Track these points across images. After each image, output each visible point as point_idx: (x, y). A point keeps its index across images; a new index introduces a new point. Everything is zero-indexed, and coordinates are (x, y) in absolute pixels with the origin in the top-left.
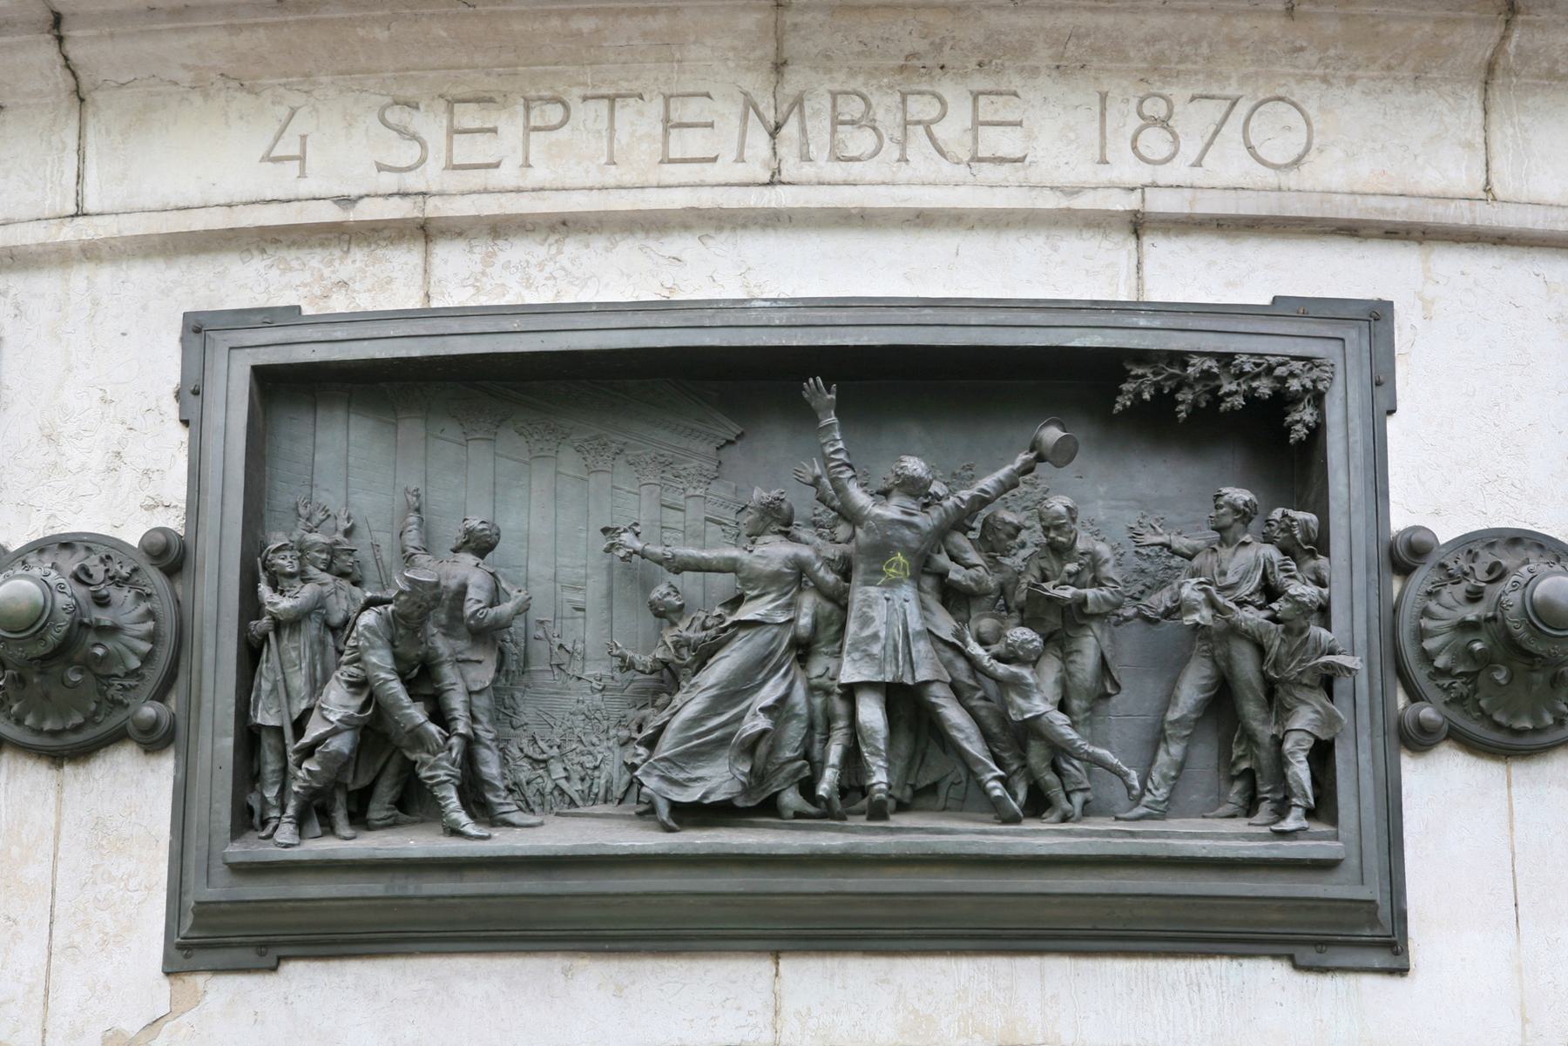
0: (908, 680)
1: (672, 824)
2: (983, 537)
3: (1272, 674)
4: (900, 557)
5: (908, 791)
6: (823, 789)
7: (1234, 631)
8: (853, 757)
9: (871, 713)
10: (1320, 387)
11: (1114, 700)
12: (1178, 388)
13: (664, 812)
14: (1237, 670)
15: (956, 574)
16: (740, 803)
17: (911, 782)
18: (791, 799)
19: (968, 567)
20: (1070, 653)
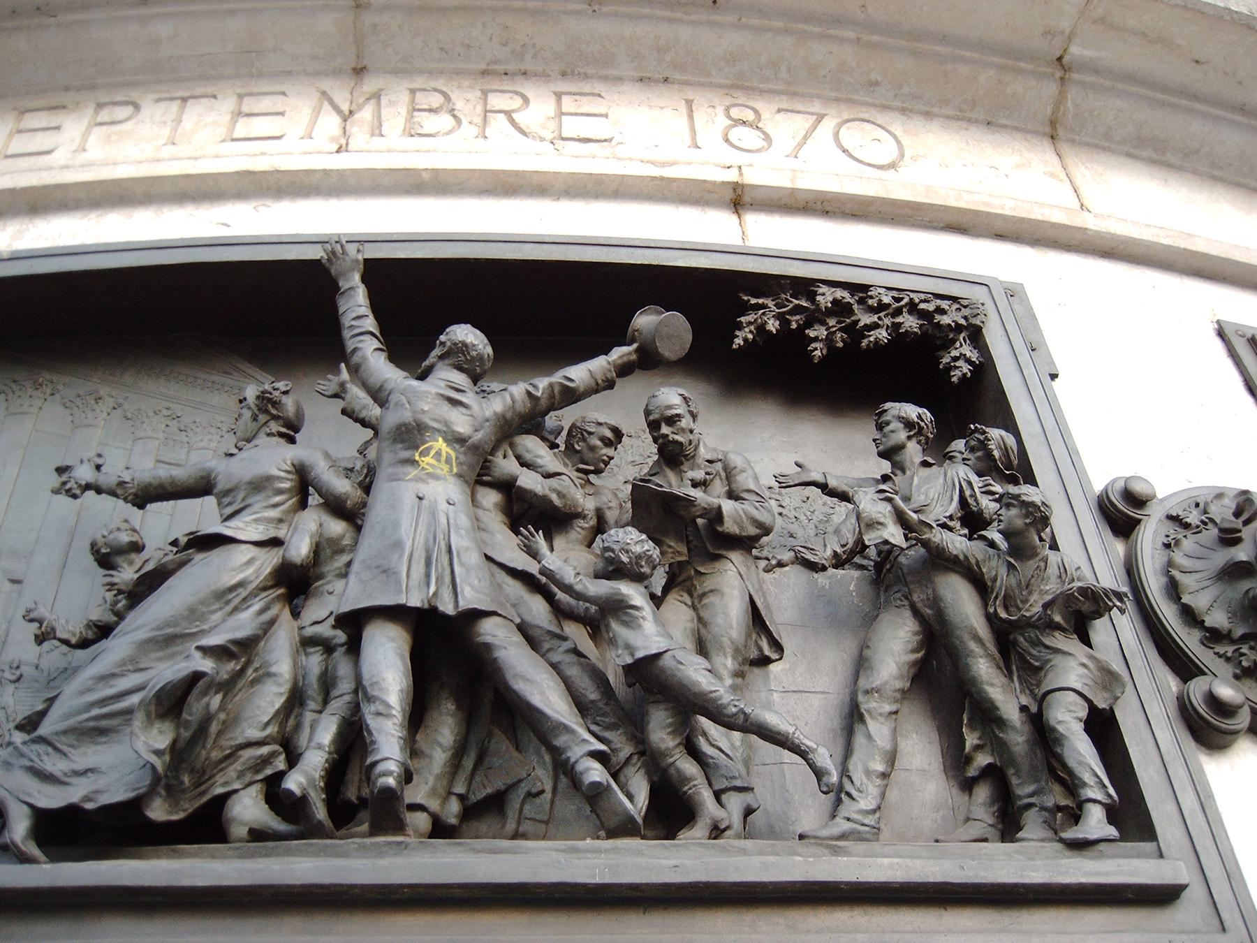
0: (447, 608)
1: (33, 849)
2: (569, 446)
3: (1003, 615)
4: (440, 444)
5: (454, 807)
7: (939, 560)
10: (977, 322)
11: (774, 668)
12: (809, 324)
13: (19, 828)
14: (951, 614)
15: (528, 481)
16: (158, 812)
17: (460, 788)
18: (249, 808)
19: (548, 476)
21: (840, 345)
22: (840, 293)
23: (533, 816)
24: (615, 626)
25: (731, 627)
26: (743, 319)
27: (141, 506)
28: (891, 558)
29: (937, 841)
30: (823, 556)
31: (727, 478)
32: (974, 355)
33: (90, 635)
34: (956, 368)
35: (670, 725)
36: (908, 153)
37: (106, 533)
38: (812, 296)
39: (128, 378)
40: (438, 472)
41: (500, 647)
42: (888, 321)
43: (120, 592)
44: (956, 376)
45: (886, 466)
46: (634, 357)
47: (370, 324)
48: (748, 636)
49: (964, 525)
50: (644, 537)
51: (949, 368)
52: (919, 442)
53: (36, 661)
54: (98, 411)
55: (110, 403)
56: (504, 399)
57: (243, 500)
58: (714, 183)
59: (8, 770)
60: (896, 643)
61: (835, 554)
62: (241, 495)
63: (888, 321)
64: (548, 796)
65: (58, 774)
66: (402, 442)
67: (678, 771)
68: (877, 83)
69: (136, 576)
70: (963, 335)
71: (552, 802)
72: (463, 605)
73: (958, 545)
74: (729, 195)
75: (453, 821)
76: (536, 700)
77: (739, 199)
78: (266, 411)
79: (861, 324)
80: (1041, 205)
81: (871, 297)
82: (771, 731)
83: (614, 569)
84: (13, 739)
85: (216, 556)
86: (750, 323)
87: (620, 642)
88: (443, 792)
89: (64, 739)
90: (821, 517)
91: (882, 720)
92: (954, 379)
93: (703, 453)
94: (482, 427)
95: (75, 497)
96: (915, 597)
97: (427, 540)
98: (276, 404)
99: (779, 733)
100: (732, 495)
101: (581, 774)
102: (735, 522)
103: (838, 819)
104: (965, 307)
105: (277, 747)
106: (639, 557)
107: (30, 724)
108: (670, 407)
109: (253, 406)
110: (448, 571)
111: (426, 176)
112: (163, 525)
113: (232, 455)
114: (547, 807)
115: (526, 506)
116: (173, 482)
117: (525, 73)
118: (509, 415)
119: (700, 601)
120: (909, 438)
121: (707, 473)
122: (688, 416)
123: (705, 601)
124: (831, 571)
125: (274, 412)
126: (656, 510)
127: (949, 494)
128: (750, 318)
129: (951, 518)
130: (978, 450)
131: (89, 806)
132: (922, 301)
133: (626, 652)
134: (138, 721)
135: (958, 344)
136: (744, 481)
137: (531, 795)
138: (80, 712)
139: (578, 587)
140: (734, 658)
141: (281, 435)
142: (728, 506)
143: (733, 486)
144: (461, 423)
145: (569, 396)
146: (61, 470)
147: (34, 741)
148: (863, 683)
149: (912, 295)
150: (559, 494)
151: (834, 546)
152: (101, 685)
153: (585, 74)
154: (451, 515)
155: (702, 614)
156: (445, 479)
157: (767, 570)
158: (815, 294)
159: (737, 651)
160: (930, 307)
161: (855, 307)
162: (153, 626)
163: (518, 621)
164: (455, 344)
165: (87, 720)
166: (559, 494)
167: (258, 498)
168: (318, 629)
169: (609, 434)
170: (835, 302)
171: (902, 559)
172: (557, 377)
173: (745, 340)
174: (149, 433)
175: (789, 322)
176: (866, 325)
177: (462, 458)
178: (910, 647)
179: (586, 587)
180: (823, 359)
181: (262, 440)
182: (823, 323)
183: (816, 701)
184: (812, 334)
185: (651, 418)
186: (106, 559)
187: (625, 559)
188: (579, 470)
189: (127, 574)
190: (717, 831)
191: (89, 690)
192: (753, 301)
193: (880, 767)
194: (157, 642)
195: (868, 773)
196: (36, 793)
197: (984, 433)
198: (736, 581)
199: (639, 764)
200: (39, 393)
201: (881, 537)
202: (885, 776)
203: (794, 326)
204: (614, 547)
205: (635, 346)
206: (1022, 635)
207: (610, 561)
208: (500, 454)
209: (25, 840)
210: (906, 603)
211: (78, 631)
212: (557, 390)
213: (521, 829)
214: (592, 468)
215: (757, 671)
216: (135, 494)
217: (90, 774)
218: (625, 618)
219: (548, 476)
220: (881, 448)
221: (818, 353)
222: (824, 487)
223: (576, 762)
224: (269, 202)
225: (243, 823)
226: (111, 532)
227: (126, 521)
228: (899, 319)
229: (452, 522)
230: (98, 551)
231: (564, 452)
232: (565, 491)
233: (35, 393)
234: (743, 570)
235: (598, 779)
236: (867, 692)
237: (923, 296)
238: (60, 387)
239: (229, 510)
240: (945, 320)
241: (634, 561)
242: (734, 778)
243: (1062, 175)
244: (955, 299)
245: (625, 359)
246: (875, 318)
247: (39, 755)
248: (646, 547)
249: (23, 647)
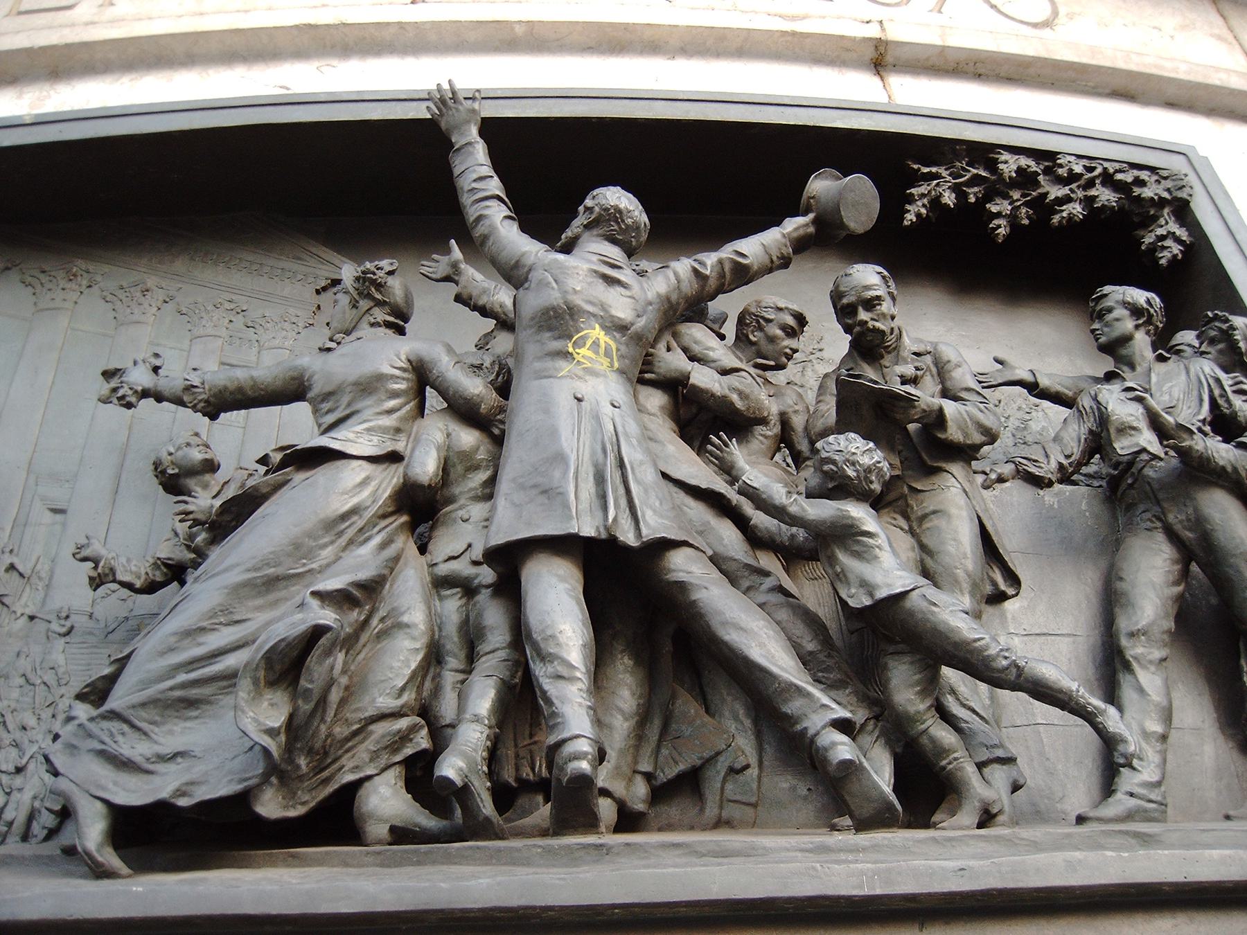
0: (628, 537)
1: (111, 858)
4: (596, 333)
5: (641, 789)
6: (450, 768)
7: (1198, 472)
8: (523, 703)
9: (558, 603)
10: (1183, 194)
11: (1010, 606)
12: (988, 197)
13: (92, 831)
14: (1221, 537)
15: (703, 378)
16: (270, 806)
17: (645, 766)
18: (387, 800)
19: (725, 372)
20: (924, 517)
21: (1026, 222)
22: (1024, 161)
23: (738, 797)
24: (843, 557)
25: (965, 557)
26: (913, 191)
27: (213, 417)
28: (1133, 470)
29: (1228, 817)
30: (1047, 469)
31: (939, 374)
32: (1182, 233)
33: (159, 578)
34: (1164, 248)
35: (918, 683)
36: (1062, 11)
37: (172, 450)
38: (992, 165)
39: (180, 265)
40: (597, 367)
41: (699, 587)
42: (1081, 194)
43: (196, 522)
44: (1164, 258)
45: (1108, 364)
46: (811, 229)
47: (495, 186)
48: (983, 568)
49: (1216, 431)
50: (871, 445)
51: (1153, 249)
52: (1148, 333)
53: (89, 609)
54: (146, 305)
55: (161, 295)
56: (668, 278)
57: (349, 405)
58: (853, 39)
59: (72, 755)
60: (1152, 573)
61: (1061, 466)
62: (345, 399)
63: (1081, 194)
64: (753, 772)
65: (138, 759)
66: (550, 329)
67: (933, 740)
69: (218, 503)
70: (1166, 211)
71: (759, 777)
72: (648, 533)
73: (1224, 455)
74: (870, 53)
75: (640, 807)
76: (756, 654)
77: (880, 58)
78: (369, 296)
79: (1052, 197)
80: (1217, 70)
81: (1061, 166)
82: (1051, 688)
83: (837, 486)
84: (73, 713)
85: (322, 475)
86: (923, 196)
87: (851, 576)
88: (628, 772)
89: (143, 714)
90: (1017, 423)
91: (1153, 668)
92: (1163, 262)
93: (909, 344)
94: (645, 311)
95: (129, 406)
96: (1171, 518)
97: (593, 453)
98: (380, 286)
99: (1061, 691)
100: (945, 394)
101: (826, 749)
102: (960, 428)
103: (1119, 796)
104: (1165, 178)
105: (418, 719)
106: (868, 470)
107: (97, 693)
108: (867, 288)
109: (352, 290)
110: (622, 491)
111: (519, 30)
112: (241, 442)
113: (329, 350)
114: (755, 786)
115: (694, 410)
116: (255, 386)
118: (674, 297)
119: (920, 525)
120: (1137, 327)
121: (917, 369)
122: (888, 299)
123: (926, 525)
124: (1057, 487)
125: (379, 297)
126: (869, 409)
127: (1195, 393)
128: (923, 189)
129: (1203, 421)
130: (1220, 342)
131: (183, 802)
132: (1117, 171)
133: (862, 591)
134: (244, 687)
135: (1162, 221)
136: (963, 377)
137: (733, 771)
138: (161, 679)
139: (793, 509)
140: (972, 594)
141: (388, 325)
142: (950, 407)
143: (949, 384)
144: (621, 306)
145: (741, 275)
146: (108, 375)
147: (104, 717)
148: (1124, 624)
149: (1106, 164)
150: (741, 394)
151: (1057, 457)
152: (186, 642)
154: (618, 420)
155: (925, 541)
156: (605, 376)
157: (986, 487)
158: (996, 162)
159: (975, 587)
160: (1128, 177)
161: (1041, 178)
162: (249, 565)
163: (710, 553)
164: (606, 210)
165: (171, 689)
166: (741, 394)
167: (368, 402)
168: (454, 566)
169: (790, 321)
170: (1020, 171)
171: (1149, 472)
172: (727, 252)
173: (918, 215)
174: (210, 331)
175: (966, 195)
176: (1057, 198)
177: (623, 348)
178: (1171, 578)
179: (803, 510)
180: (1007, 238)
181: (365, 331)
182: (1006, 196)
183: (1064, 645)
184: (994, 209)
185: (845, 301)
186: (174, 482)
187: (851, 472)
188: (757, 366)
189: (205, 500)
190: (987, 818)
191: (171, 650)
192: (926, 170)
193: (1156, 727)
194: (255, 586)
195: (1146, 735)
196: (111, 786)
197: (1227, 321)
198: (961, 500)
199: (876, 733)
200: (73, 285)
201: (1138, 444)
202: (1164, 738)
203: (972, 199)
204: (837, 458)
205: (811, 216)
207: (828, 476)
208: (662, 346)
209: (100, 847)
210: (1159, 524)
211: (143, 572)
212: (727, 267)
213: (725, 814)
214: (772, 363)
215: (989, 611)
216: (207, 401)
217: (179, 760)
218: (856, 548)
219: (725, 372)
220: (1103, 339)
221: (1002, 231)
222: (1033, 388)
223: (817, 734)
224: (335, 62)
225: (381, 820)
226: (179, 448)
227: (197, 434)
228: (1093, 192)
229: (620, 429)
230: (163, 472)
231: (735, 344)
232: (747, 391)
233: (68, 285)
234: (967, 486)
235: (848, 757)
236: (1132, 635)
237: (1117, 166)
238: (99, 278)
239: (330, 419)
240: (1147, 193)
241: (863, 474)
242: (995, 746)
243: (1230, 37)
244: (1153, 170)
245: (801, 232)
246: (1066, 190)
247: (112, 735)
248: (876, 458)
249: (73, 592)
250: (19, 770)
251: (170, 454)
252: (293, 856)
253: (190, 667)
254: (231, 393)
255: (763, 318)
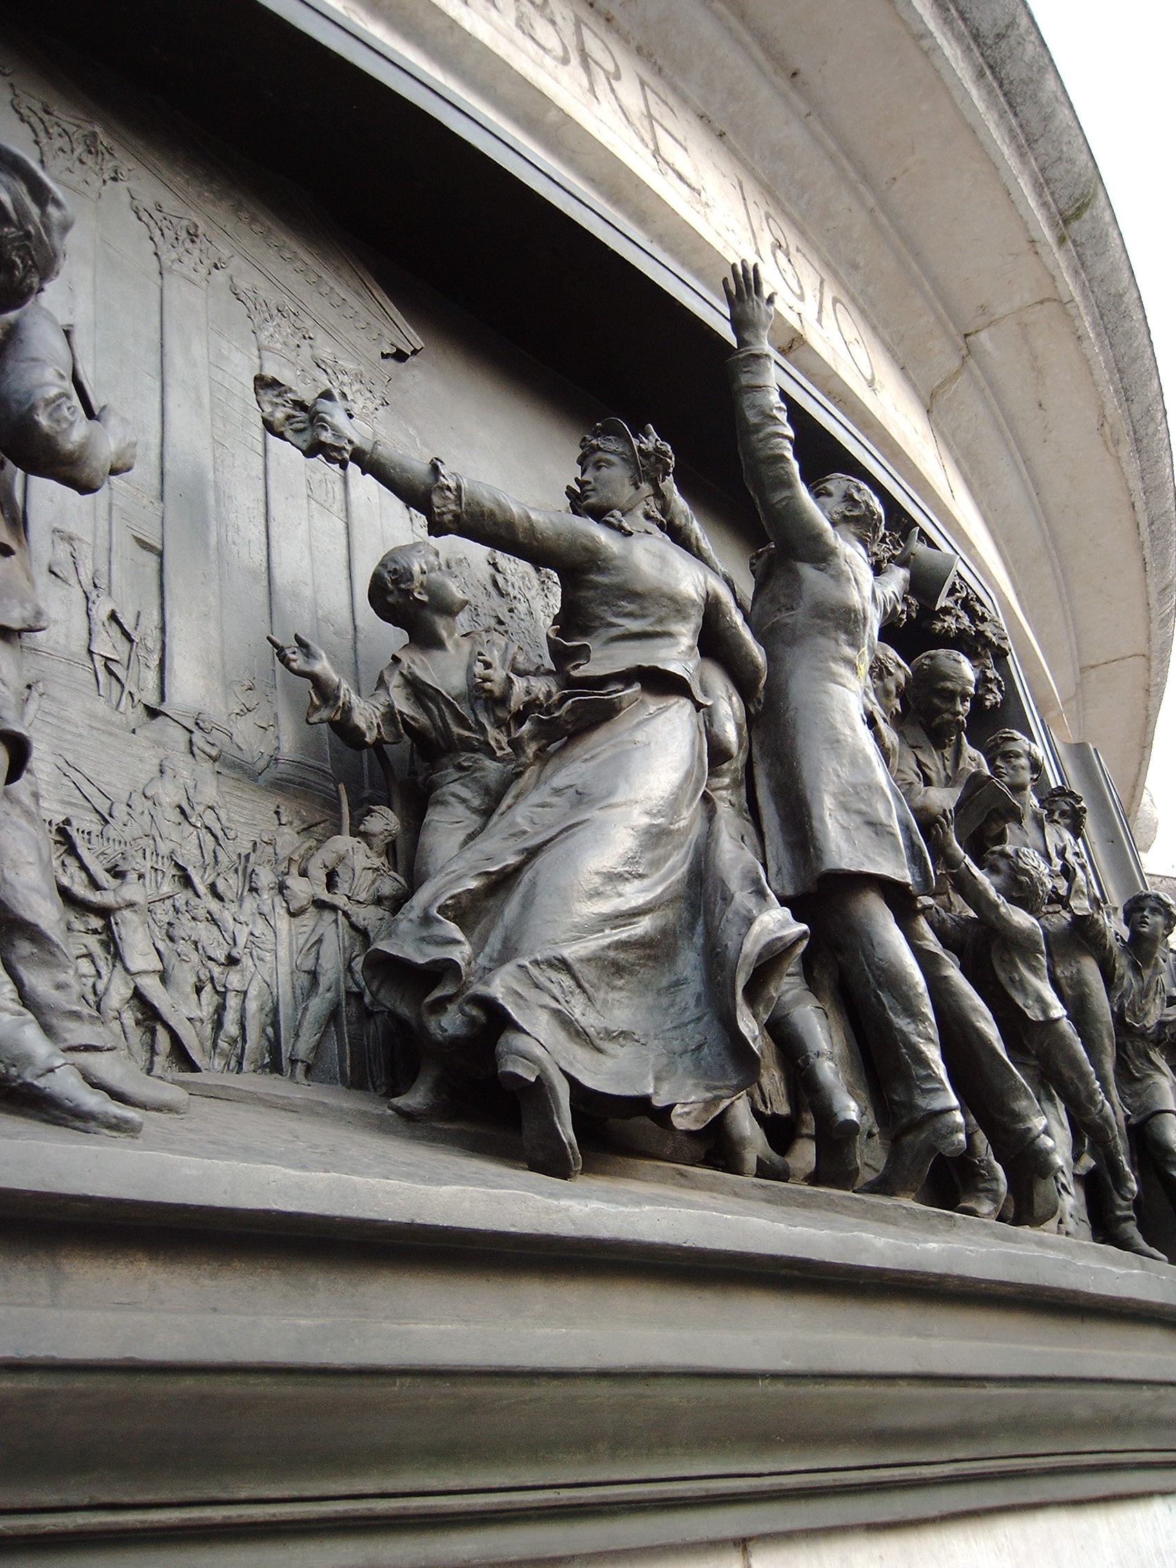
65: (591, 1031)
68: (855, 267)
92: (988, 703)
96: (1058, 971)
117: (608, 20)
133: (1036, 1006)
153: (660, 70)
206: (1132, 1042)
226: (432, 570)
233: (89, 160)
250: (232, 961)
251: (423, 572)
252: (682, 1174)
253: (618, 922)
254: (496, 523)
255: (887, 668)
